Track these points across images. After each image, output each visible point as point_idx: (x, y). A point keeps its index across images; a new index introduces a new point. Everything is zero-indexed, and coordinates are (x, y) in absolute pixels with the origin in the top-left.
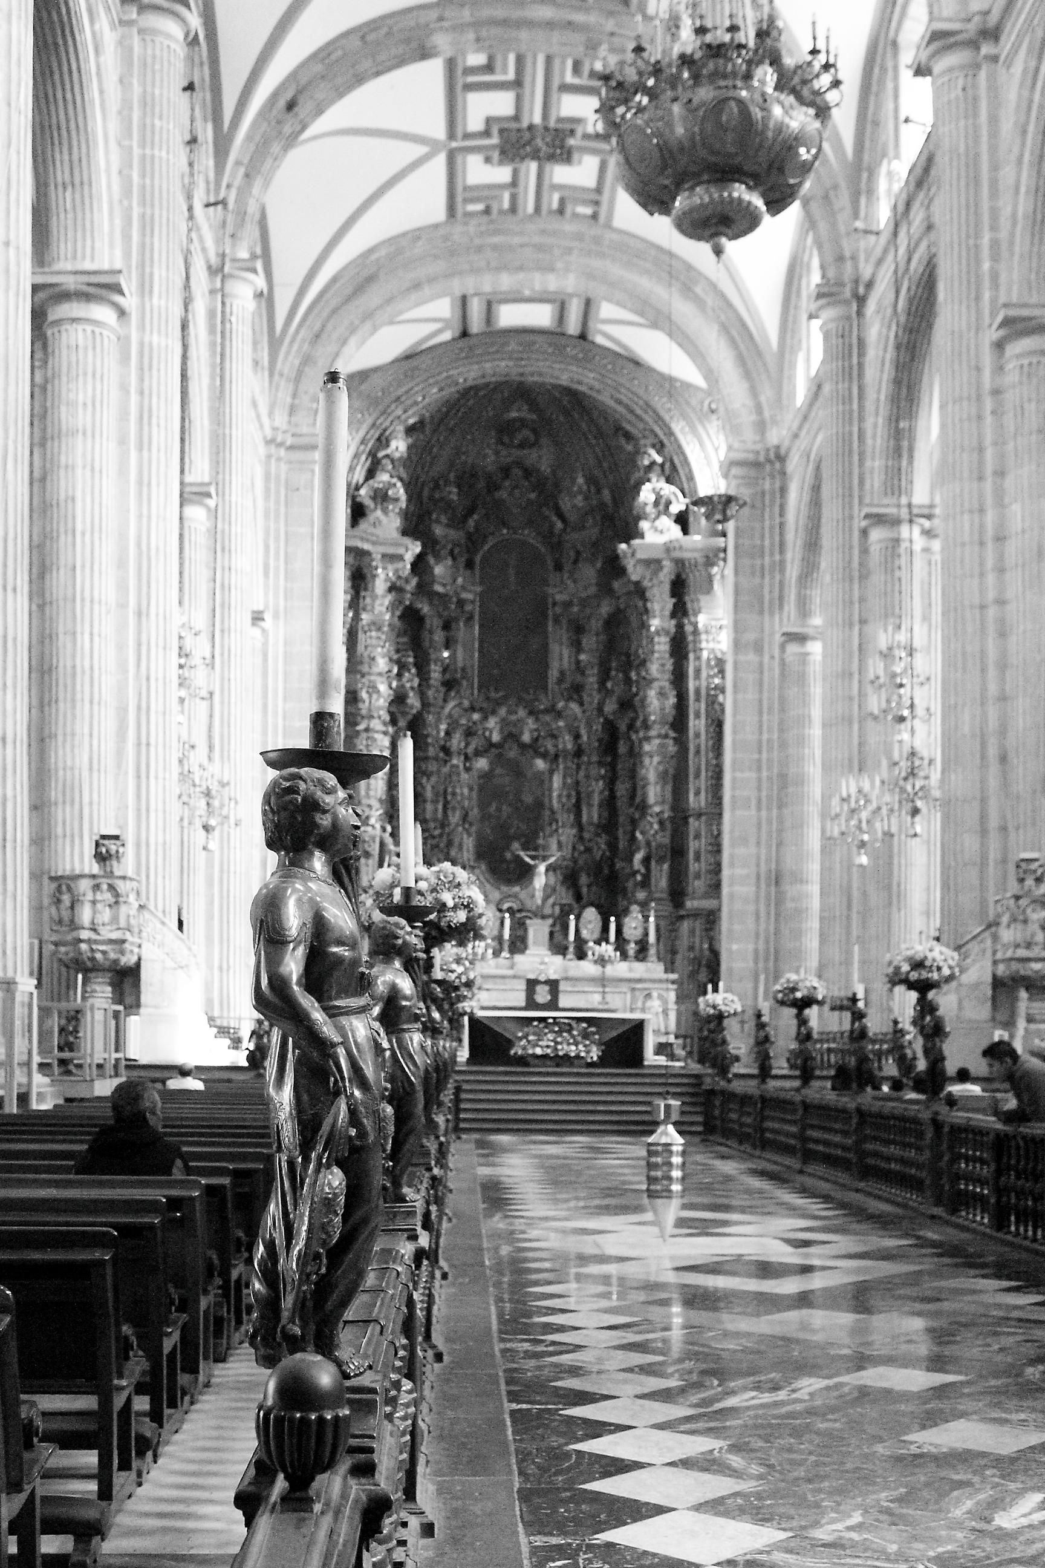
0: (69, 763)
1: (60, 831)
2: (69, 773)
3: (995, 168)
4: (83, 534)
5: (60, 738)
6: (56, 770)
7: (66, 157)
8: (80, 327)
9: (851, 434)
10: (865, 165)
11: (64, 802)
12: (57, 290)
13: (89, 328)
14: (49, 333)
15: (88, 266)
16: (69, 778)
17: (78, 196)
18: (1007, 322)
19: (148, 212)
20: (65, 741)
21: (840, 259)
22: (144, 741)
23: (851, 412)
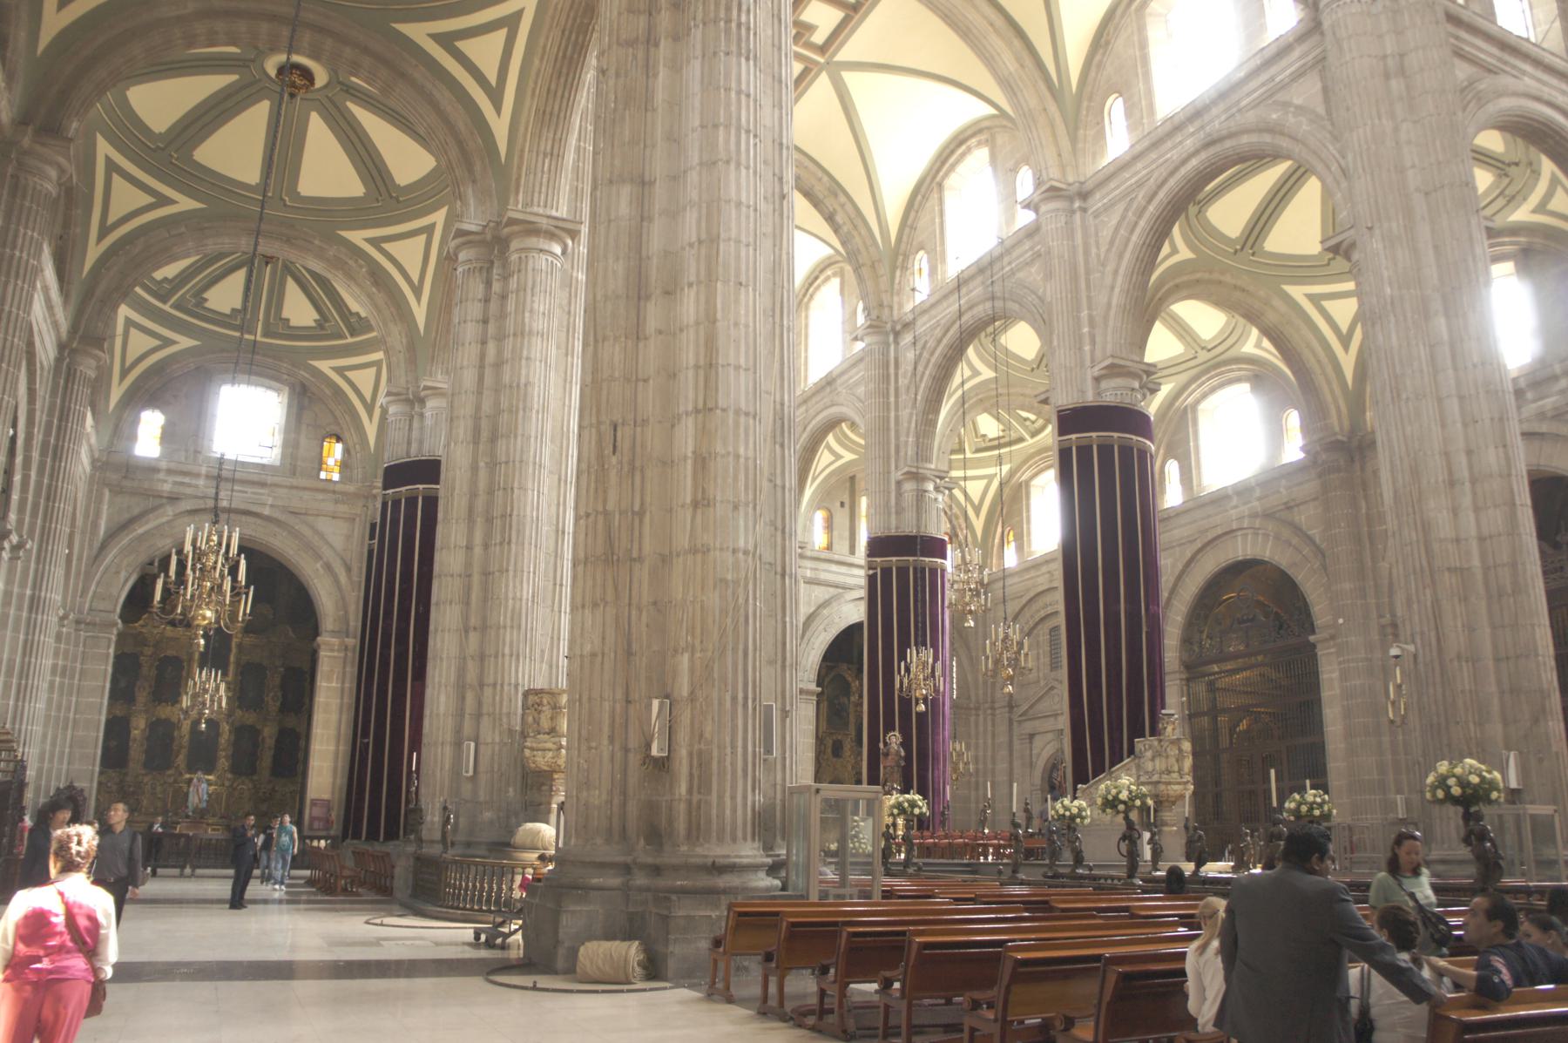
0: (518, 594)
1: (507, 651)
2: (518, 603)
3: (1088, 273)
4: (538, 412)
5: (511, 573)
6: (506, 599)
7: (551, 135)
8: (544, 257)
9: (888, 418)
10: (901, 251)
11: (512, 627)
12: (531, 226)
13: (550, 259)
14: (514, 257)
15: (554, 213)
16: (517, 606)
17: (554, 163)
18: (1112, 366)
19: (580, 186)
20: (515, 576)
21: (881, 305)
22: (558, 582)
23: (888, 404)
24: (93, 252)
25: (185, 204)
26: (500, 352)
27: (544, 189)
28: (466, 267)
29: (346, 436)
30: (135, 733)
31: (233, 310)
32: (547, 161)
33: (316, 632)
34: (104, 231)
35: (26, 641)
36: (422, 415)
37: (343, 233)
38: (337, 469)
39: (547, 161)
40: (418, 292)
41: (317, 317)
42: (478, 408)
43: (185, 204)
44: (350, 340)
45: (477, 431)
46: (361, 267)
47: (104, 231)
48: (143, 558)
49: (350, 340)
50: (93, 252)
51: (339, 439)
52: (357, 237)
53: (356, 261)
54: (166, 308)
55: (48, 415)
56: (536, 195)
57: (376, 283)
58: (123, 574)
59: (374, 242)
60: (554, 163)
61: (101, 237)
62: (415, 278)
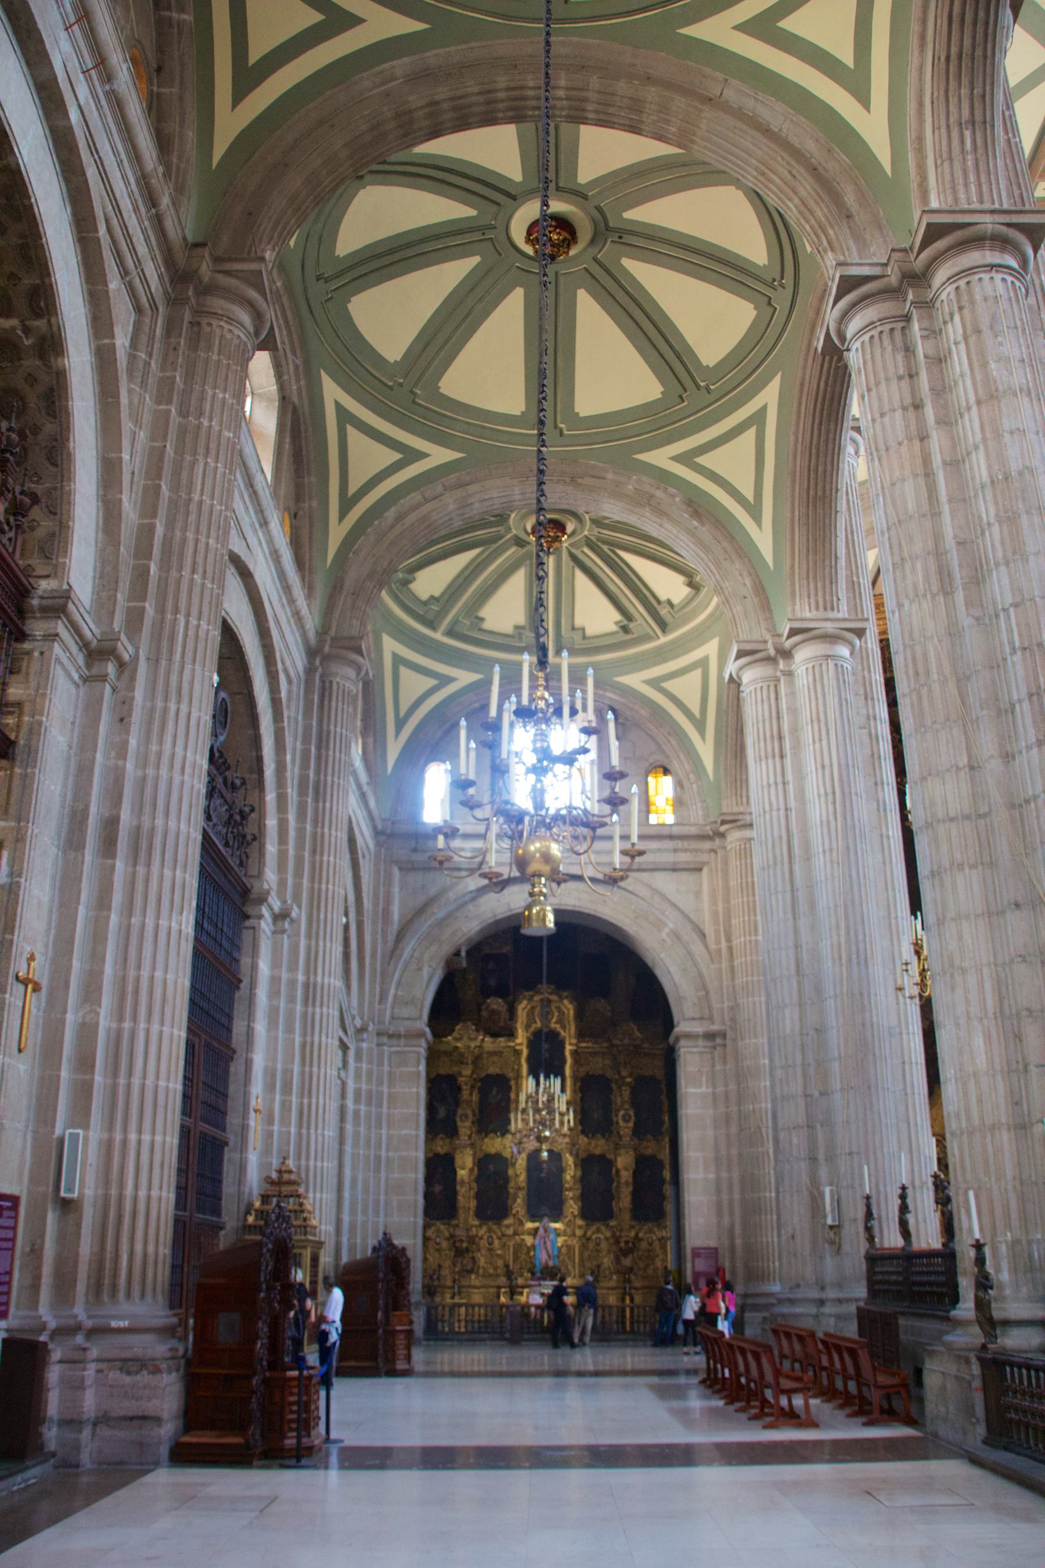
17: (979, 135)
24: (337, 533)
25: (439, 455)
26: (954, 442)
27: (972, 178)
28: (866, 337)
29: (675, 765)
30: (462, 1173)
31: (517, 627)
32: (968, 134)
33: (669, 1023)
34: (347, 504)
35: (303, 1045)
36: (789, 674)
37: (640, 457)
38: (670, 809)
39: (968, 134)
40: (755, 511)
41: (617, 616)
42: (938, 537)
43: (439, 455)
44: (664, 639)
45: (944, 574)
46: (673, 496)
47: (347, 504)
48: (447, 949)
49: (664, 639)
50: (337, 533)
51: (666, 771)
52: (660, 457)
53: (665, 491)
54: (438, 636)
55: (303, 742)
56: (961, 189)
57: (696, 514)
58: (426, 971)
59: (686, 459)
60: (979, 135)
61: (343, 514)
62: (749, 494)
